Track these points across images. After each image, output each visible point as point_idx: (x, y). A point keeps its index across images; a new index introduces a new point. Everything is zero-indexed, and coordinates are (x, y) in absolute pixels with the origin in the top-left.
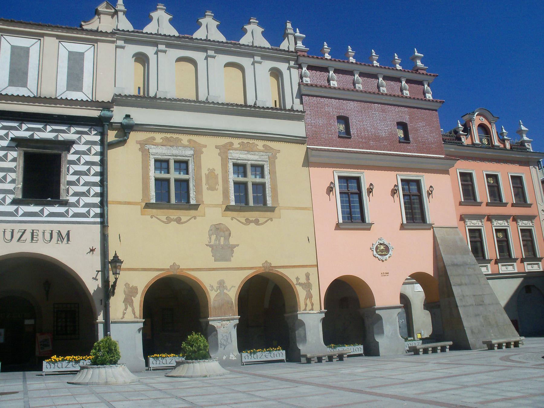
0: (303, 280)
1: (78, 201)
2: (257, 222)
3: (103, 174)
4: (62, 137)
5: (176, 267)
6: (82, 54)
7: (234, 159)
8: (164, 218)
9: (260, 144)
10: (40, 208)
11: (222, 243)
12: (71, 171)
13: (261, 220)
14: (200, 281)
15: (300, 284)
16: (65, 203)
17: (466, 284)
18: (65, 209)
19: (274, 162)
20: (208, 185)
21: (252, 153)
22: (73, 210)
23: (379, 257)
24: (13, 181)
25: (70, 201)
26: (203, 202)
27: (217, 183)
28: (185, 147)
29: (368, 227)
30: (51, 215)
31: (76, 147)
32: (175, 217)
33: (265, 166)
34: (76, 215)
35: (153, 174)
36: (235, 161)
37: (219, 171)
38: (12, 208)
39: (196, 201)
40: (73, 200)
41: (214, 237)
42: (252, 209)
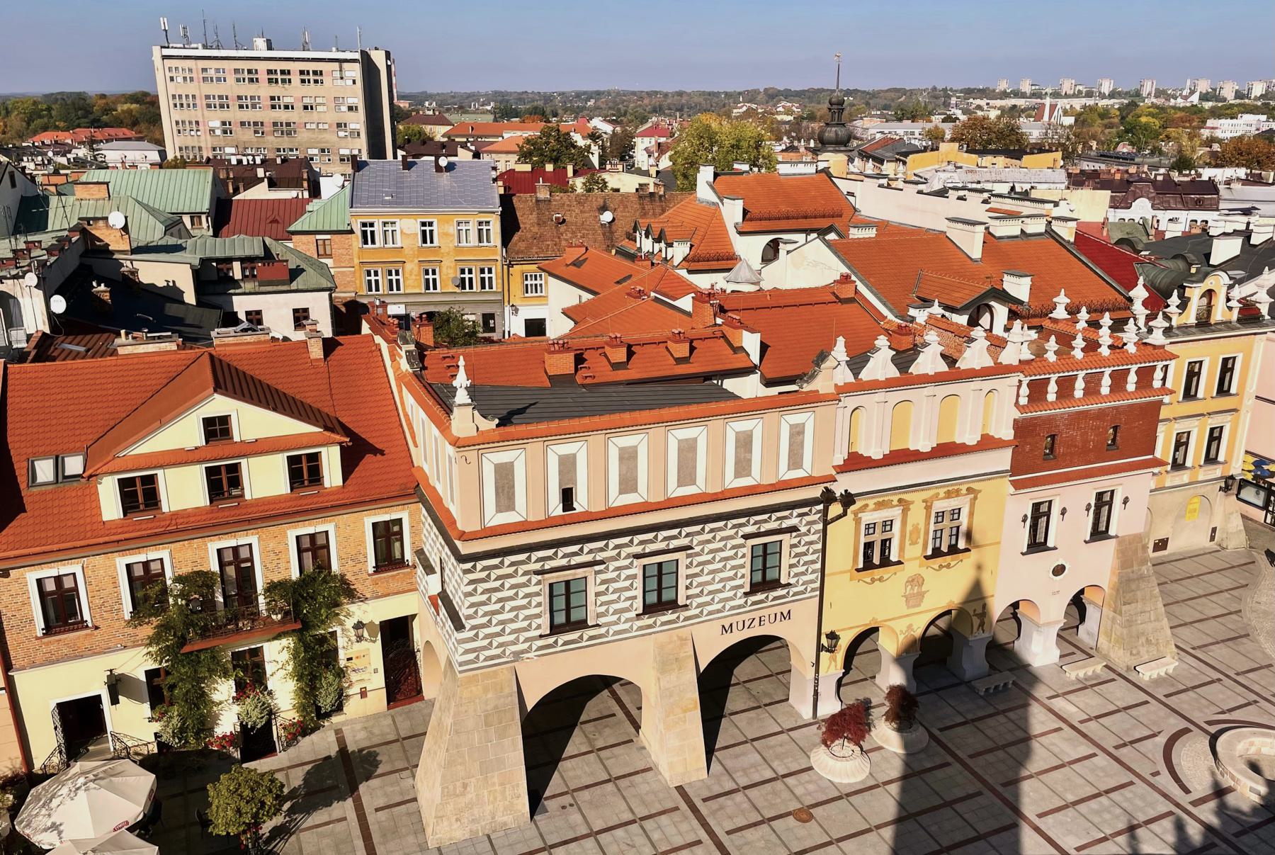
0: (979, 611)
2: (948, 566)
8: (868, 580)
10: (765, 595)
18: (786, 591)
27: (919, 537)
30: (775, 598)
37: (922, 526)
40: (792, 581)
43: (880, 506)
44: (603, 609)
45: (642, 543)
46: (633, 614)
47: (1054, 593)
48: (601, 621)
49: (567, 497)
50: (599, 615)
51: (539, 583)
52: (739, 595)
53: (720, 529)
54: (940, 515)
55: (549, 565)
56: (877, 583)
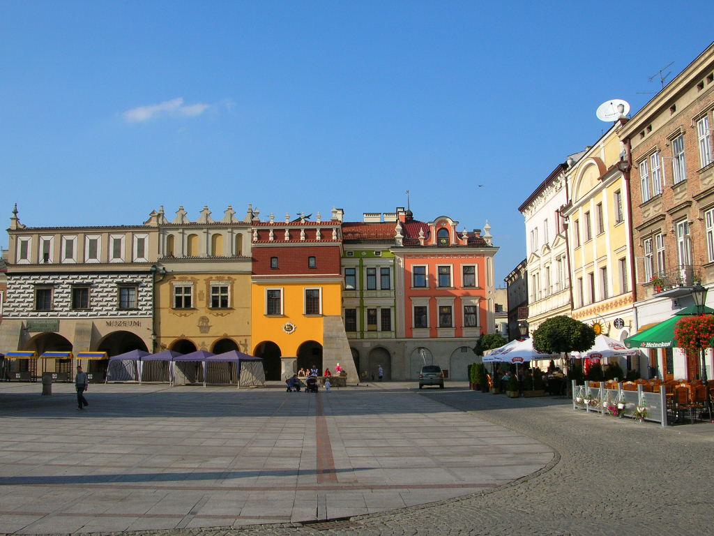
0: (243, 342)
6: (144, 239)
9: (226, 276)
16: (138, 310)
22: (140, 312)
24: (116, 301)
34: (141, 314)
37: (205, 292)
38: (116, 313)
40: (140, 308)
42: (219, 309)
45: (72, 279)
46: (68, 309)
48: (56, 309)
49: (46, 256)
50: (55, 306)
53: (105, 278)
54: (215, 290)
55: (37, 282)
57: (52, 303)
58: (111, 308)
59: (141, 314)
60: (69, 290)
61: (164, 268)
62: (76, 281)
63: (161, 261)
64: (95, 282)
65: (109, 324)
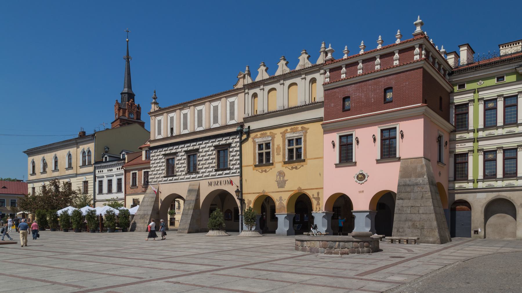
0: (316, 196)
1: (233, 168)
2: (296, 168)
3: (241, 155)
4: (228, 142)
5: (264, 192)
7: (288, 138)
8: (260, 171)
9: (300, 127)
10: (222, 172)
11: (281, 180)
12: (231, 155)
13: (298, 167)
14: (273, 198)
15: (314, 198)
16: (230, 169)
17: (410, 199)
19: (306, 135)
20: (277, 153)
21: (296, 132)
22: (232, 171)
23: (358, 182)
25: (231, 168)
26: (275, 161)
28: (268, 136)
29: (355, 164)
30: (226, 174)
31: (233, 145)
32: (264, 170)
33: (302, 138)
34: (233, 173)
35: (257, 151)
36: (288, 138)
37: (281, 146)
38: (214, 173)
39: (272, 161)
40: (231, 167)
41: (278, 177)
42: (294, 162)
43: (262, 136)
44: (177, 170)
46: (184, 173)
47: (360, 192)
48: (178, 174)
49: (172, 129)
50: (177, 172)
51: (164, 159)
52: (214, 170)
54: (290, 142)
56: (264, 172)
57: (175, 169)
58: (211, 169)
59: (233, 173)
60: (185, 157)
61: (249, 127)
62: (190, 148)
63: (247, 120)
64: (201, 147)
65: (210, 184)
